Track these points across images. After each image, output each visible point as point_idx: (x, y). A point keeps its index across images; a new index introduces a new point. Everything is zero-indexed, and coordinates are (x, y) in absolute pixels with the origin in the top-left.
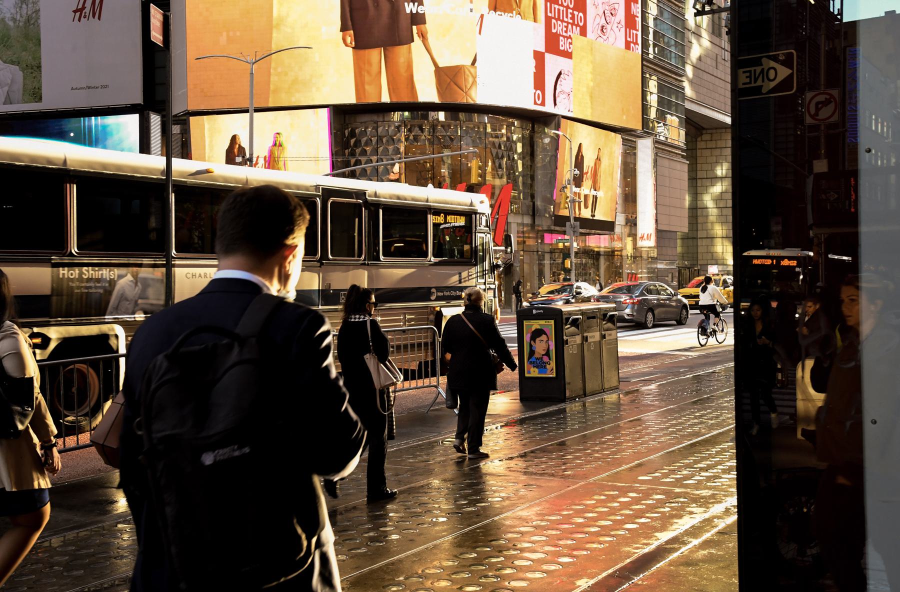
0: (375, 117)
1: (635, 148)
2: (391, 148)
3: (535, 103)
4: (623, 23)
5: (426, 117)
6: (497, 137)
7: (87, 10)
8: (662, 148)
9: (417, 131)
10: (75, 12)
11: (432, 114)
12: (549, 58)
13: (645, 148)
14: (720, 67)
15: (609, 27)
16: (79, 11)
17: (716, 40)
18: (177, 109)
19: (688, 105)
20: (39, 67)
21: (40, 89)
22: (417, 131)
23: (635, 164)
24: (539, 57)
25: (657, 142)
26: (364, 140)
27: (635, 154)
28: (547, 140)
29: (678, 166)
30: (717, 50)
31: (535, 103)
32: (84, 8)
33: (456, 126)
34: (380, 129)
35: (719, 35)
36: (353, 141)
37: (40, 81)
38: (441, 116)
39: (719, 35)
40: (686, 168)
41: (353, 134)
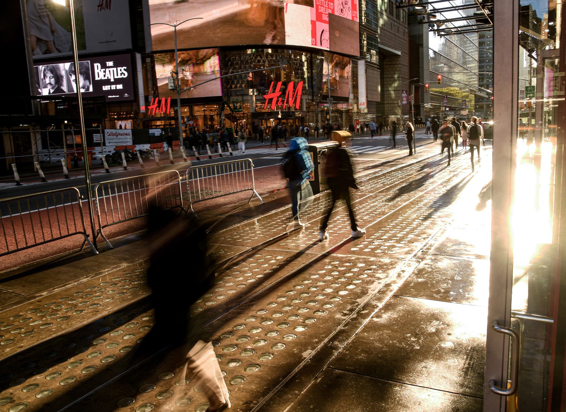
0: (239, 52)
1: (357, 64)
2: (247, 66)
3: (312, 44)
4: (351, 8)
5: (263, 51)
6: (295, 60)
7: (104, 5)
8: (369, 65)
9: (259, 58)
10: (98, 6)
11: (265, 50)
12: (318, 23)
13: (361, 65)
14: (393, 29)
15: (344, 10)
16: (100, 6)
17: (391, 17)
18: (148, 51)
19: (380, 45)
20: (84, 33)
21: (85, 43)
22: (259, 58)
23: (357, 72)
24: (313, 23)
25: (366, 62)
26: (235, 62)
27: (357, 67)
28: (318, 61)
29: (376, 72)
30: (392, 21)
31: (312, 44)
32: (102, 4)
33: (276, 56)
34: (242, 57)
35: (392, 15)
36: (230, 63)
37: (85, 40)
38: (270, 51)
39: (392, 15)
40: (379, 73)
41: (229, 60)
